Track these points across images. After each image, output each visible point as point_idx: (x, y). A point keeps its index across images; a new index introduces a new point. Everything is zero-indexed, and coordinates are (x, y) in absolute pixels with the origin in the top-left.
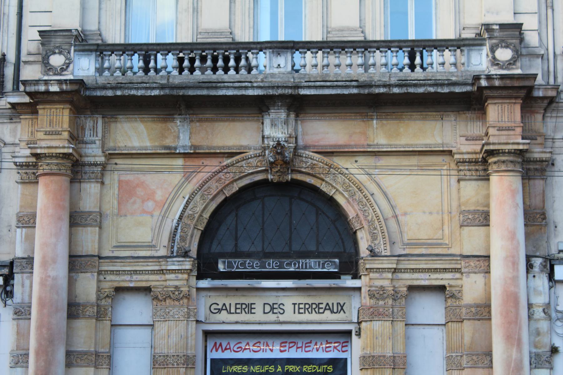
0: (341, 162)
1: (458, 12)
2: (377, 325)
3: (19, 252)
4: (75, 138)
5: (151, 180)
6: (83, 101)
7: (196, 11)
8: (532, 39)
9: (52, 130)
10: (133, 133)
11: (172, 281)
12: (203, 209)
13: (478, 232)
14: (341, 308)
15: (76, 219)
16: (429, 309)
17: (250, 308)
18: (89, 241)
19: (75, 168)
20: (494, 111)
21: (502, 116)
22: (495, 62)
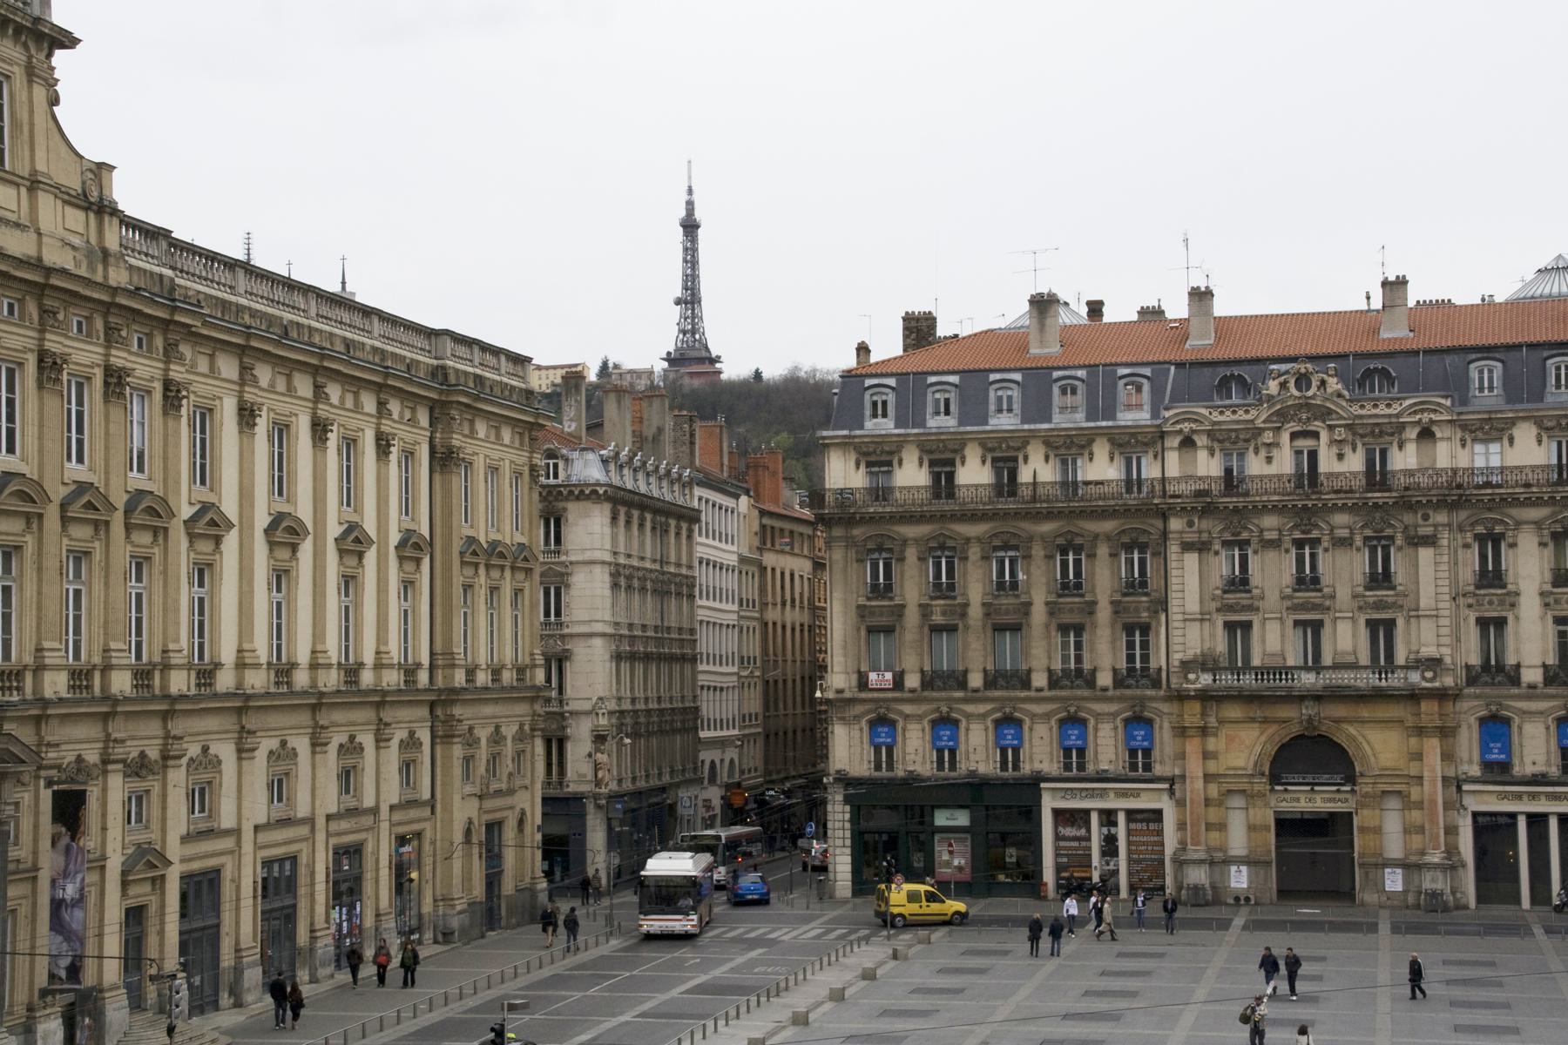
0: (1345, 726)
1: (1408, 643)
2: (1366, 812)
3: (1177, 772)
4: (1204, 714)
5: (1243, 734)
6: (1205, 696)
7: (1264, 641)
8: (1448, 660)
9: (1192, 714)
10: (1234, 711)
11: (1256, 787)
12: (1272, 750)
13: (1417, 763)
14: (1347, 800)
15: (1207, 755)
16: (1393, 803)
17: (1298, 800)
18: (1212, 767)
19: (1204, 731)
20: (1423, 705)
21: (1428, 707)
22: (1424, 678)
